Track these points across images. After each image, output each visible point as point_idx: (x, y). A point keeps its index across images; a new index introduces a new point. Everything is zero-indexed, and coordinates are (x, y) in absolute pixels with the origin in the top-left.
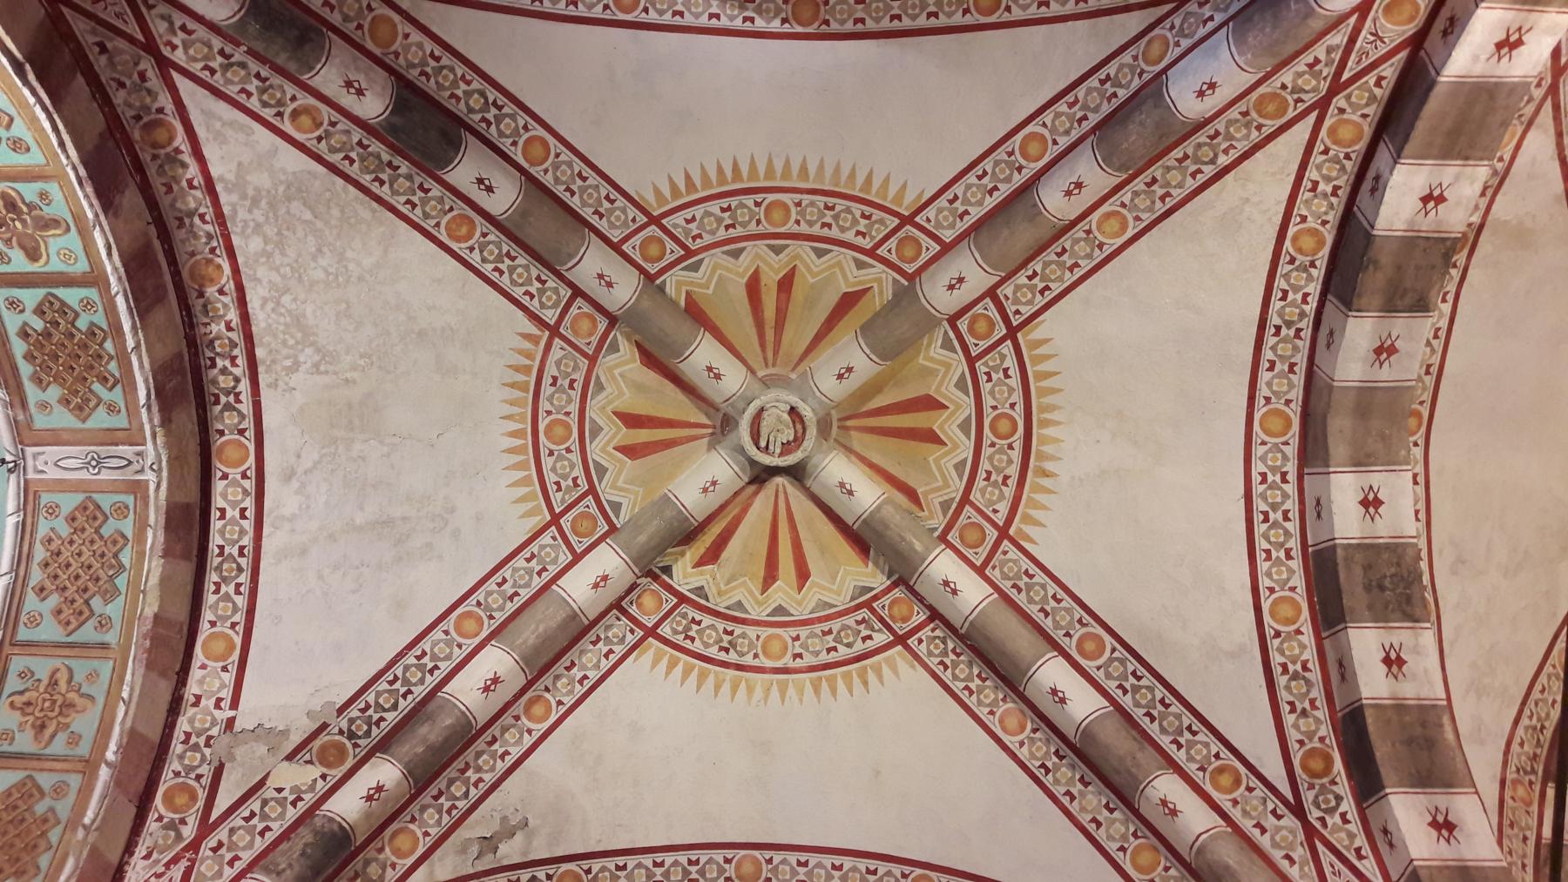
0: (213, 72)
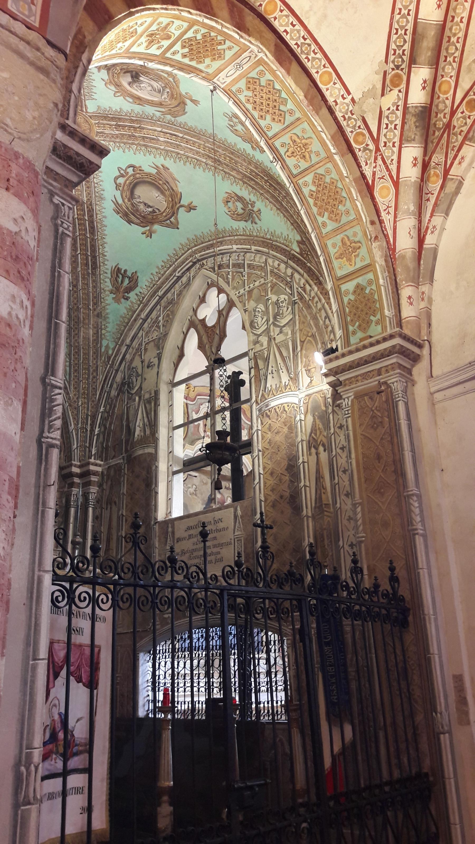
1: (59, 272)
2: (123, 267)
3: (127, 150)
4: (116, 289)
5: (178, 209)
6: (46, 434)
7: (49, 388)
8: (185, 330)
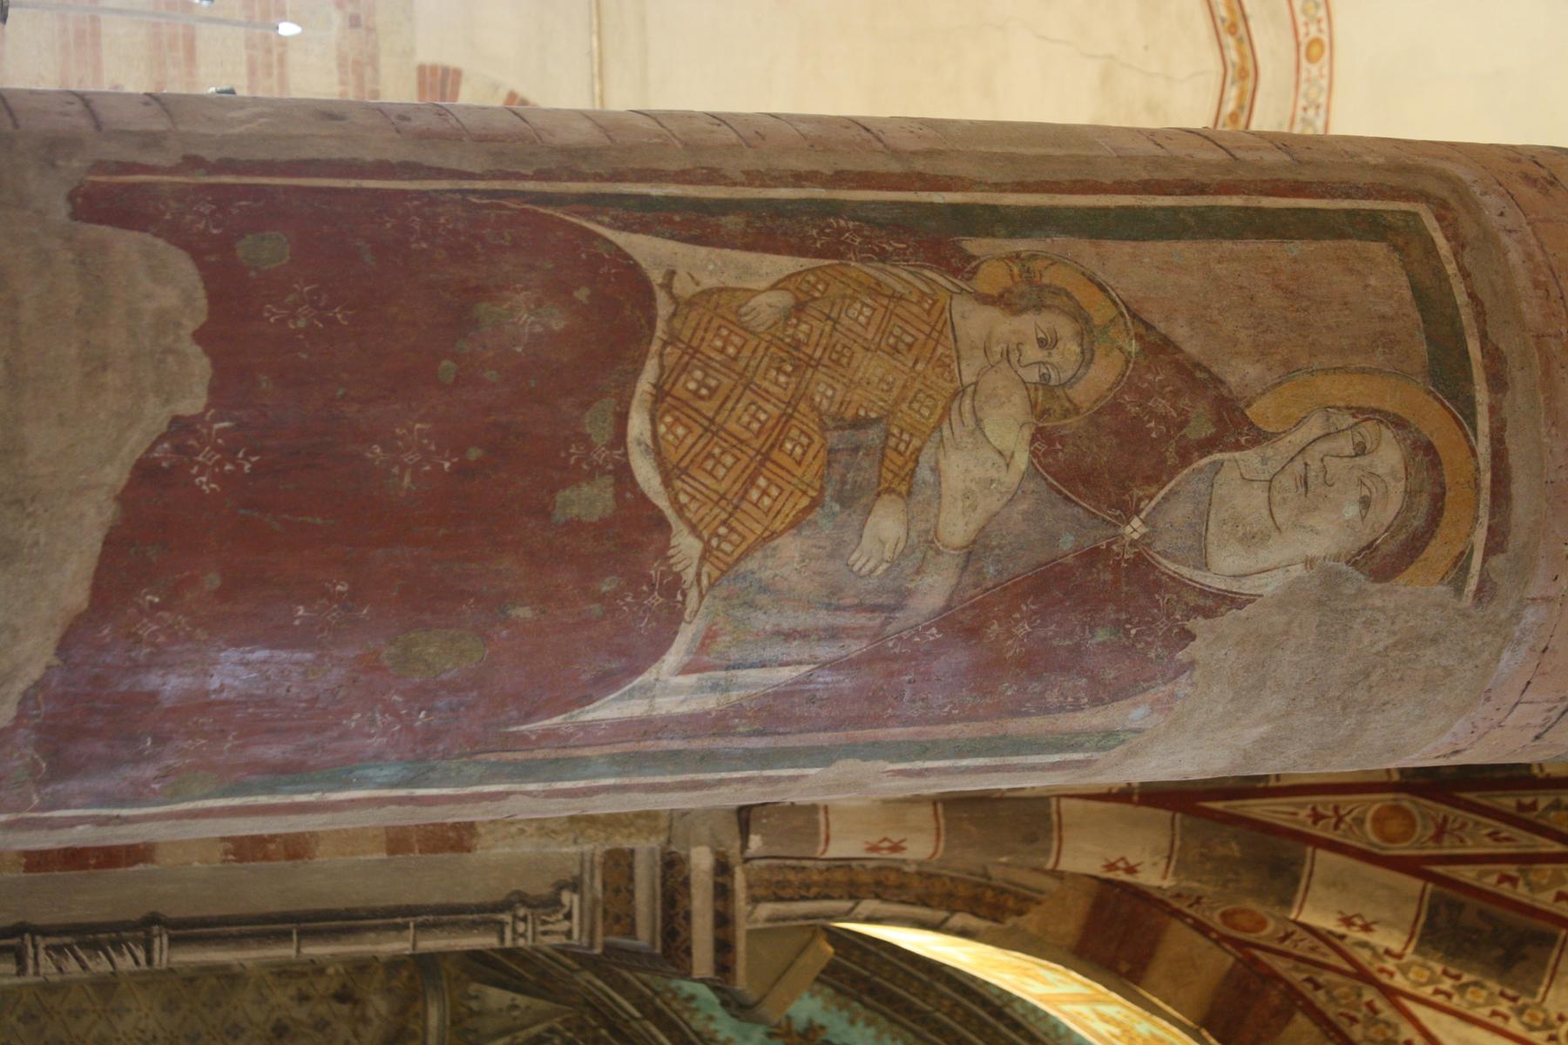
0: (1449, 996)
1: (406, 927)
6: (42, 942)
7: (141, 934)
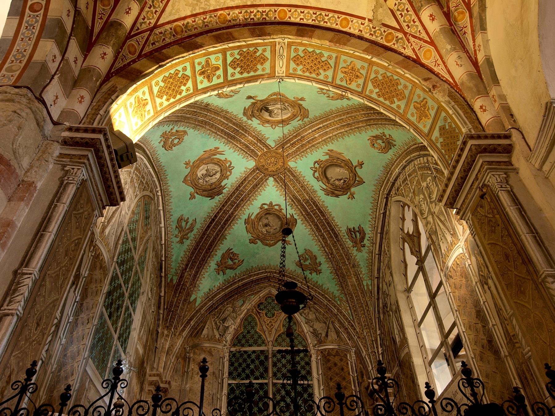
2: (351, 226)
3: (307, 155)
4: (355, 243)
5: (355, 170)
8: (401, 247)
